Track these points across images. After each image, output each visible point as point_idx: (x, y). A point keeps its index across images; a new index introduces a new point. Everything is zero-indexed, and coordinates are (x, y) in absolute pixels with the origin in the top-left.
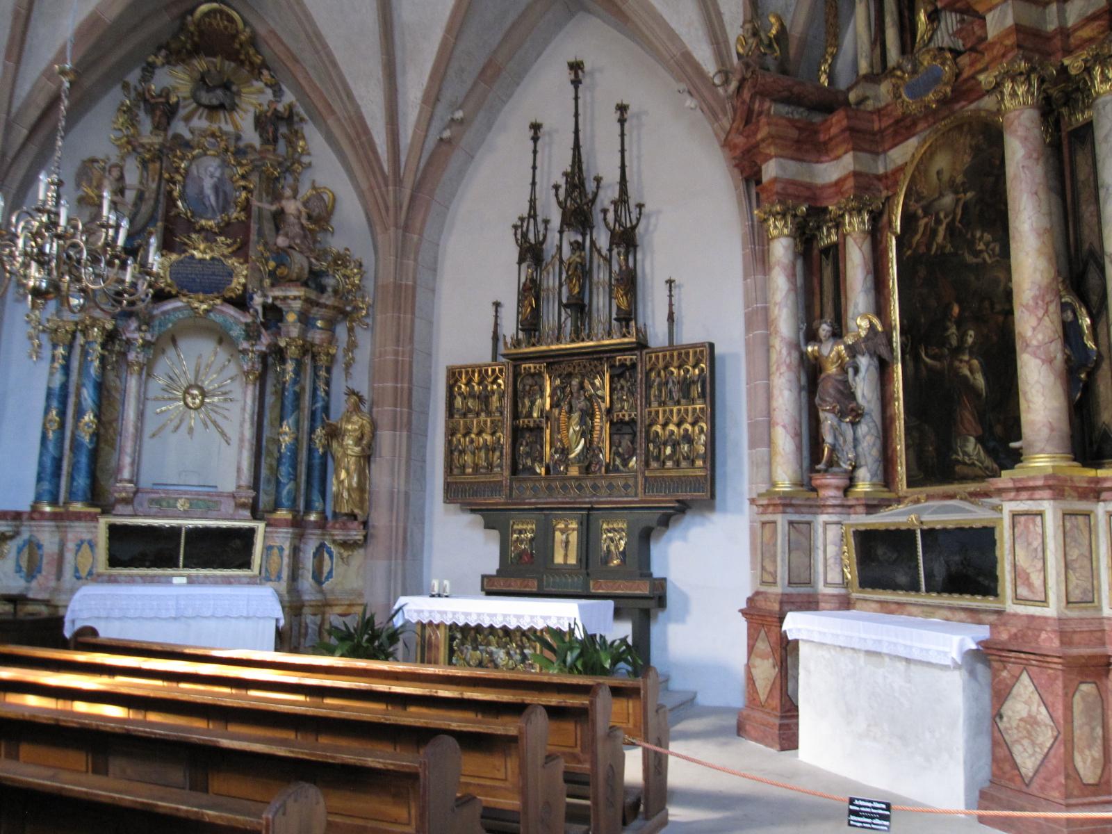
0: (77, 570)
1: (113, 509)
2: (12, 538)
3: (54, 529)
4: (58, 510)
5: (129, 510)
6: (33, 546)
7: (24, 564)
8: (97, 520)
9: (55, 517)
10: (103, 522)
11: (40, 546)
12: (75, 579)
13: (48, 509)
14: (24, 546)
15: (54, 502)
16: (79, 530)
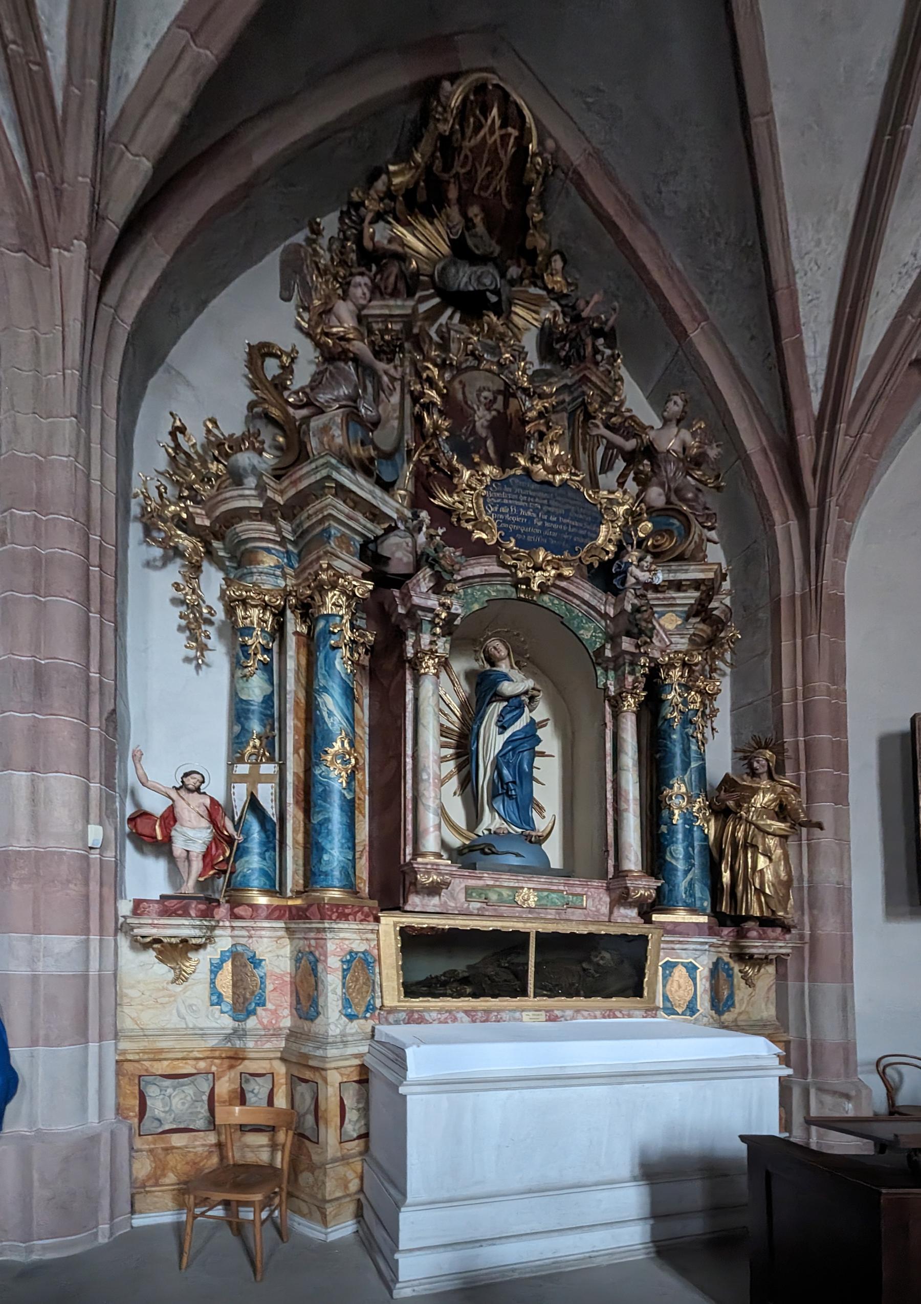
0: (347, 1002)
1: (405, 902)
2: (198, 947)
3: (282, 933)
4: (282, 902)
5: (433, 903)
6: (243, 962)
7: (227, 991)
8: (377, 920)
9: (274, 913)
10: (389, 923)
11: (256, 963)
12: (344, 1019)
13: (263, 900)
14: (223, 961)
15: (274, 887)
16: (344, 938)
